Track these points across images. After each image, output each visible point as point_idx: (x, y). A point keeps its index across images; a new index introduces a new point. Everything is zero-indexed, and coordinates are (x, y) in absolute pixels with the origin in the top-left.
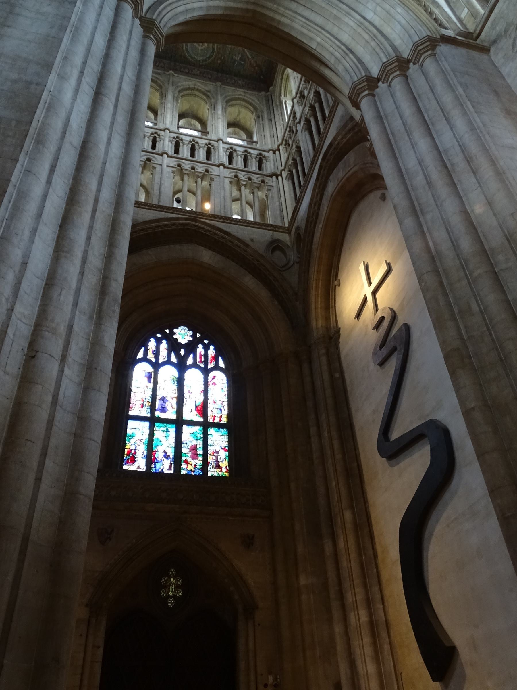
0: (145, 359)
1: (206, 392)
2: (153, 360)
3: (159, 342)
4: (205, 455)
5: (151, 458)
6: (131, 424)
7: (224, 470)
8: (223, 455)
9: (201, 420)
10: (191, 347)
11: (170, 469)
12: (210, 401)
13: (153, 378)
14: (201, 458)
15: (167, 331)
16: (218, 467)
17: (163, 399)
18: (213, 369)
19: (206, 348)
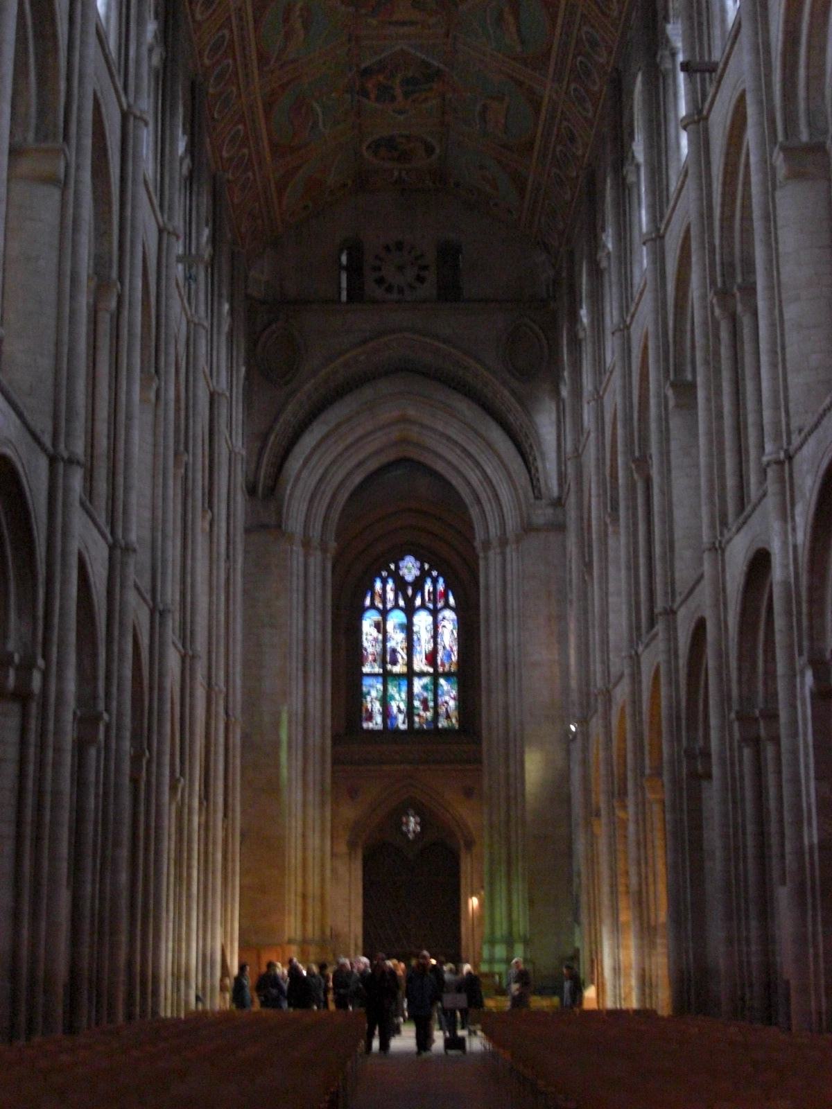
0: (373, 606)
3: (384, 583)
4: (436, 706)
5: (386, 713)
6: (367, 682)
7: (454, 721)
8: (452, 703)
9: (431, 670)
10: (418, 585)
11: (404, 723)
12: (440, 647)
13: (380, 627)
14: (431, 710)
16: (448, 717)
17: (394, 651)
19: (435, 582)
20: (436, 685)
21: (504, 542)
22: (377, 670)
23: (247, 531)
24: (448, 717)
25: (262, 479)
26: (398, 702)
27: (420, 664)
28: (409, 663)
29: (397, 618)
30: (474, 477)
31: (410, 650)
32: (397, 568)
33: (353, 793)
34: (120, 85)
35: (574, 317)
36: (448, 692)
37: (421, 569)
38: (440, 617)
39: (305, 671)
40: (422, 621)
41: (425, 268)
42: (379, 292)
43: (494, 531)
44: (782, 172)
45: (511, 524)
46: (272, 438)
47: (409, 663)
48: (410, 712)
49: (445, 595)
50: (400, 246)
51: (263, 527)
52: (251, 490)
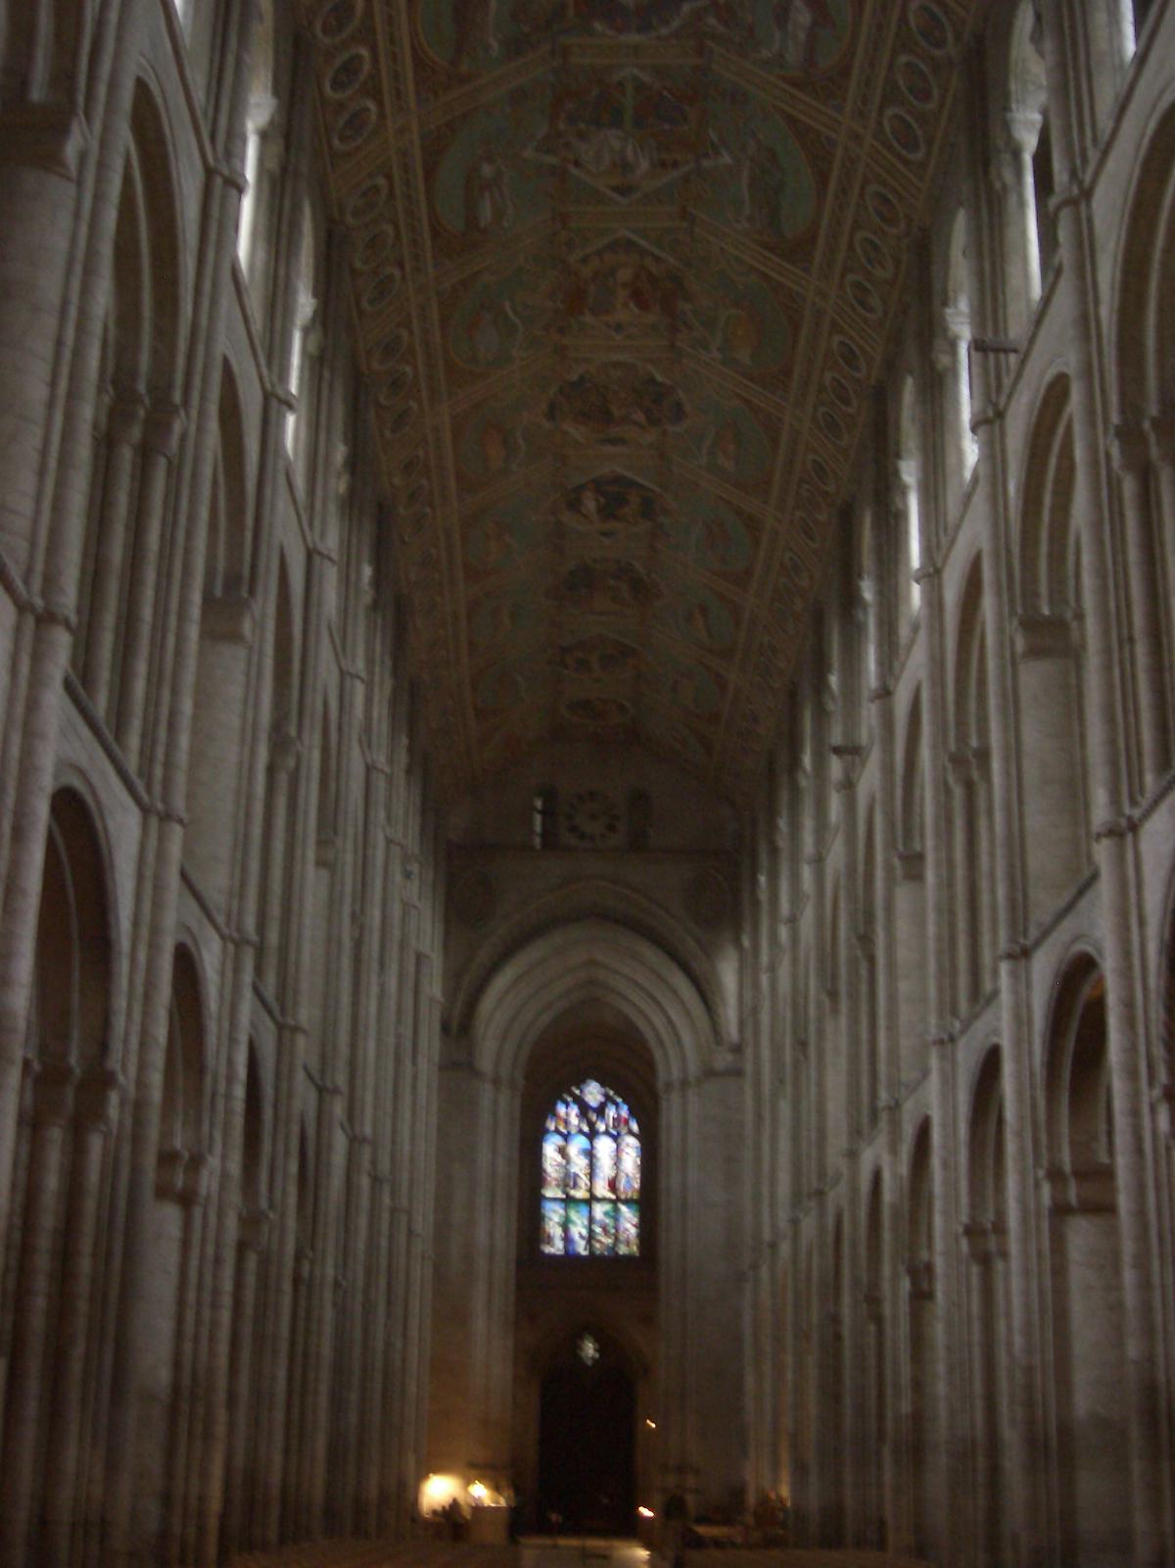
2: (564, 1131)
5: (567, 1239)
7: (635, 1248)
8: (633, 1231)
9: (613, 1197)
11: (585, 1249)
12: (622, 1175)
20: (616, 1210)
21: (685, 1084)
22: (560, 1195)
23: (442, 1068)
24: (628, 1243)
26: (578, 1229)
27: (602, 1189)
29: (578, 1143)
30: (658, 1020)
31: (592, 1174)
35: (754, 882)
37: (606, 1095)
40: (604, 1146)
43: (676, 1074)
44: (899, 872)
45: (693, 1069)
47: (590, 1190)
48: (591, 1237)
49: (626, 1122)
52: (445, 1028)
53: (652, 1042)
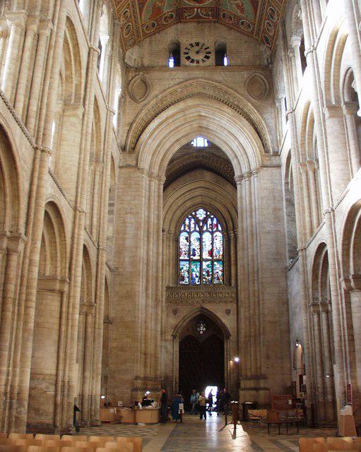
0: (185, 231)
1: (212, 244)
3: (190, 220)
5: (191, 278)
6: (182, 263)
8: (220, 273)
9: (211, 258)
10: (205, 221)
12: (215, 248)
15: (194, 213)
16: (218, 279)
18: (216, 231)
19: (212, 220)
20: (213, 264)
21: (250, 174)
22: (186, 258)
24: (218, 279)
25: (129, 143)
27: (206, 255)
28: (201, 255)
29: (195, 235)
30: (234, 145)
32: (196, 214)
33: (175, 312)
34: (88, 38)
36: (218, 267)
37: (206, 214)
38: (215, 235)
39: (148, 237)
41: (210, 53)
42: (188, 63)
45: (253, 166)
46: (134, 125)
47: (201, 255)
48: (201, 277)
49: (217, 226)
50: (197, 44)
51: (128, 166)
53: (231, 156)
